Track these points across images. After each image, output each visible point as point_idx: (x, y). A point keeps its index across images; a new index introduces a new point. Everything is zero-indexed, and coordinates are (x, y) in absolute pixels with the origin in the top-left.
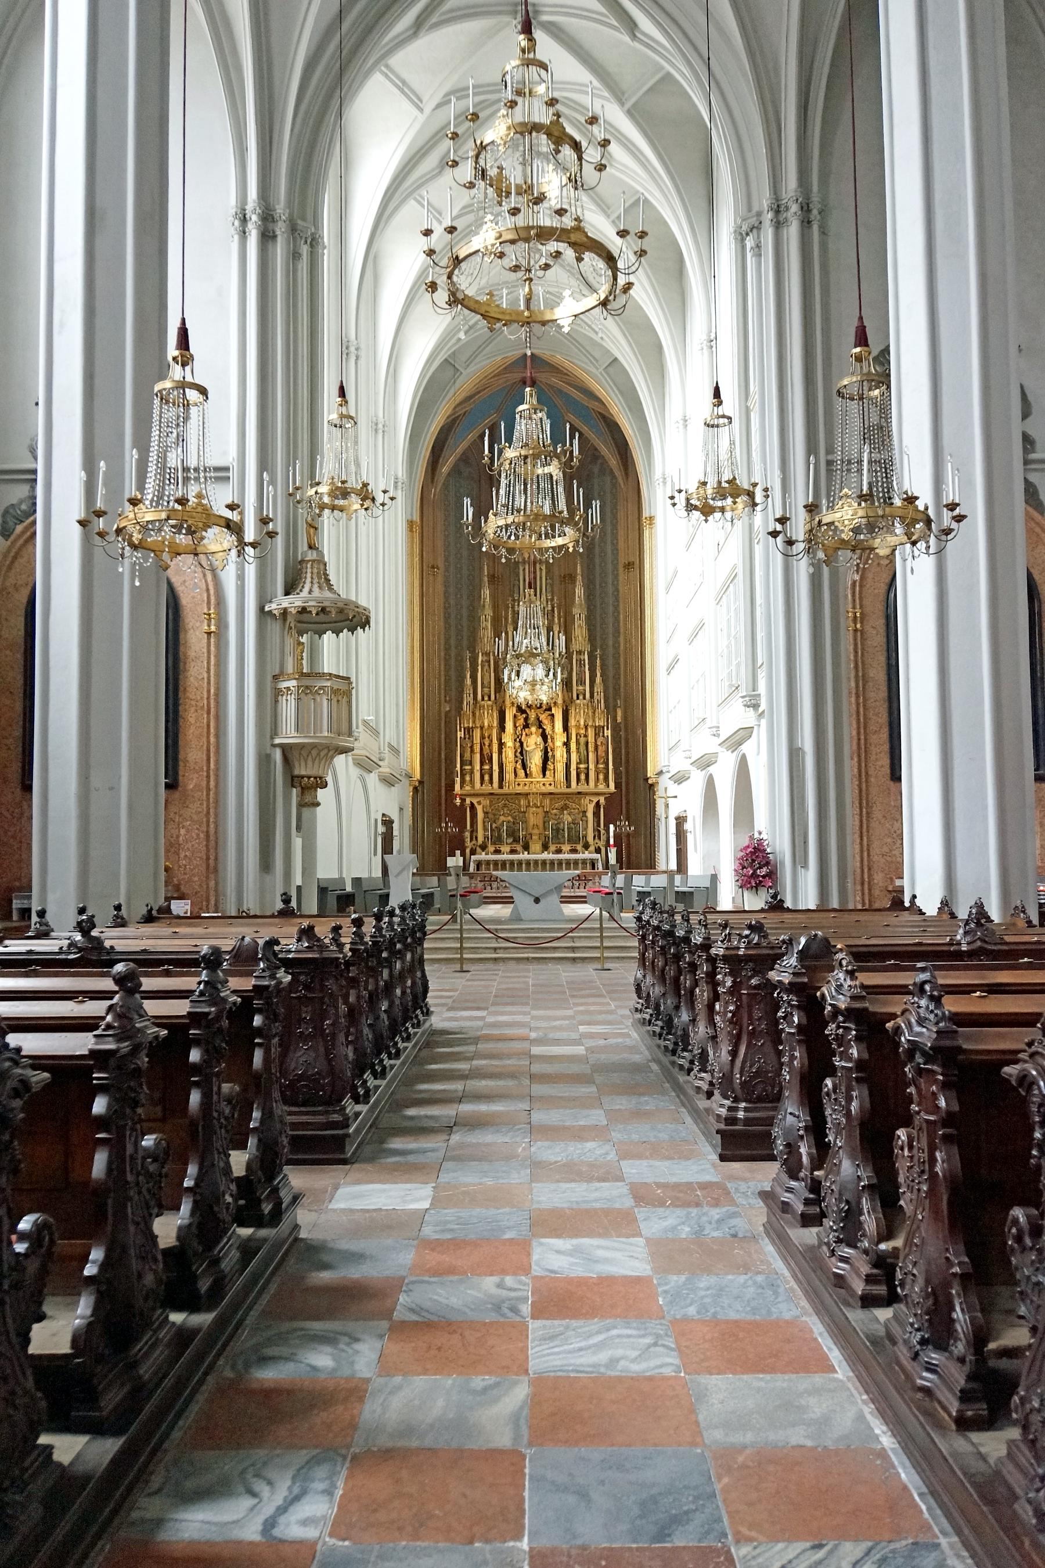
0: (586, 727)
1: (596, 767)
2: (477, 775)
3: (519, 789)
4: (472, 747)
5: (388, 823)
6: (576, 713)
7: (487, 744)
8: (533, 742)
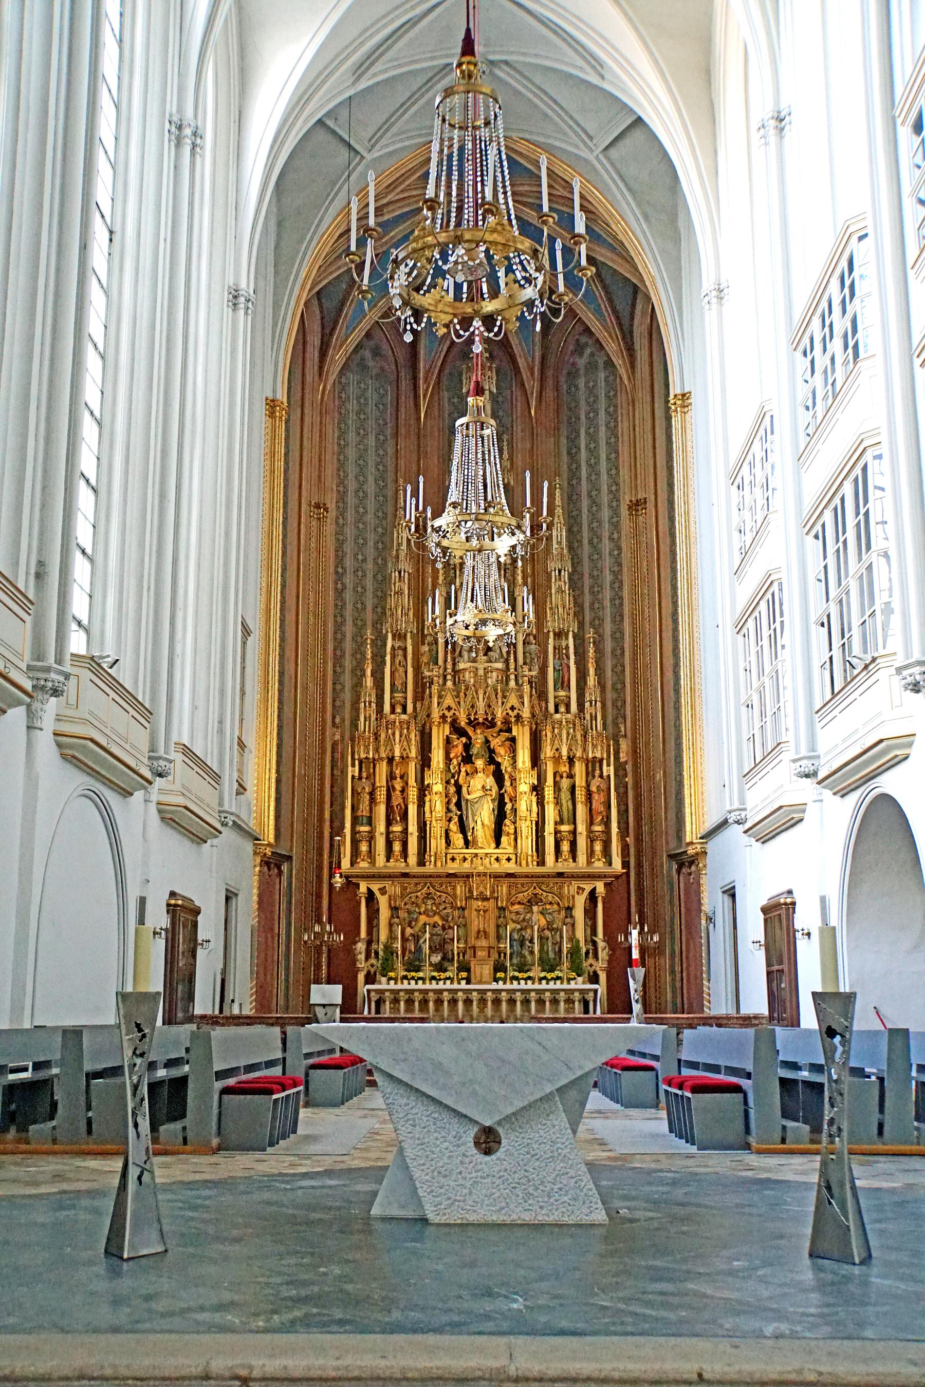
0: (571, 761)
1: (590, 831)
2: (380, 842)
3: (453, 868)
4: (372, 794)
5: (183, 914)
7: (398, 787)
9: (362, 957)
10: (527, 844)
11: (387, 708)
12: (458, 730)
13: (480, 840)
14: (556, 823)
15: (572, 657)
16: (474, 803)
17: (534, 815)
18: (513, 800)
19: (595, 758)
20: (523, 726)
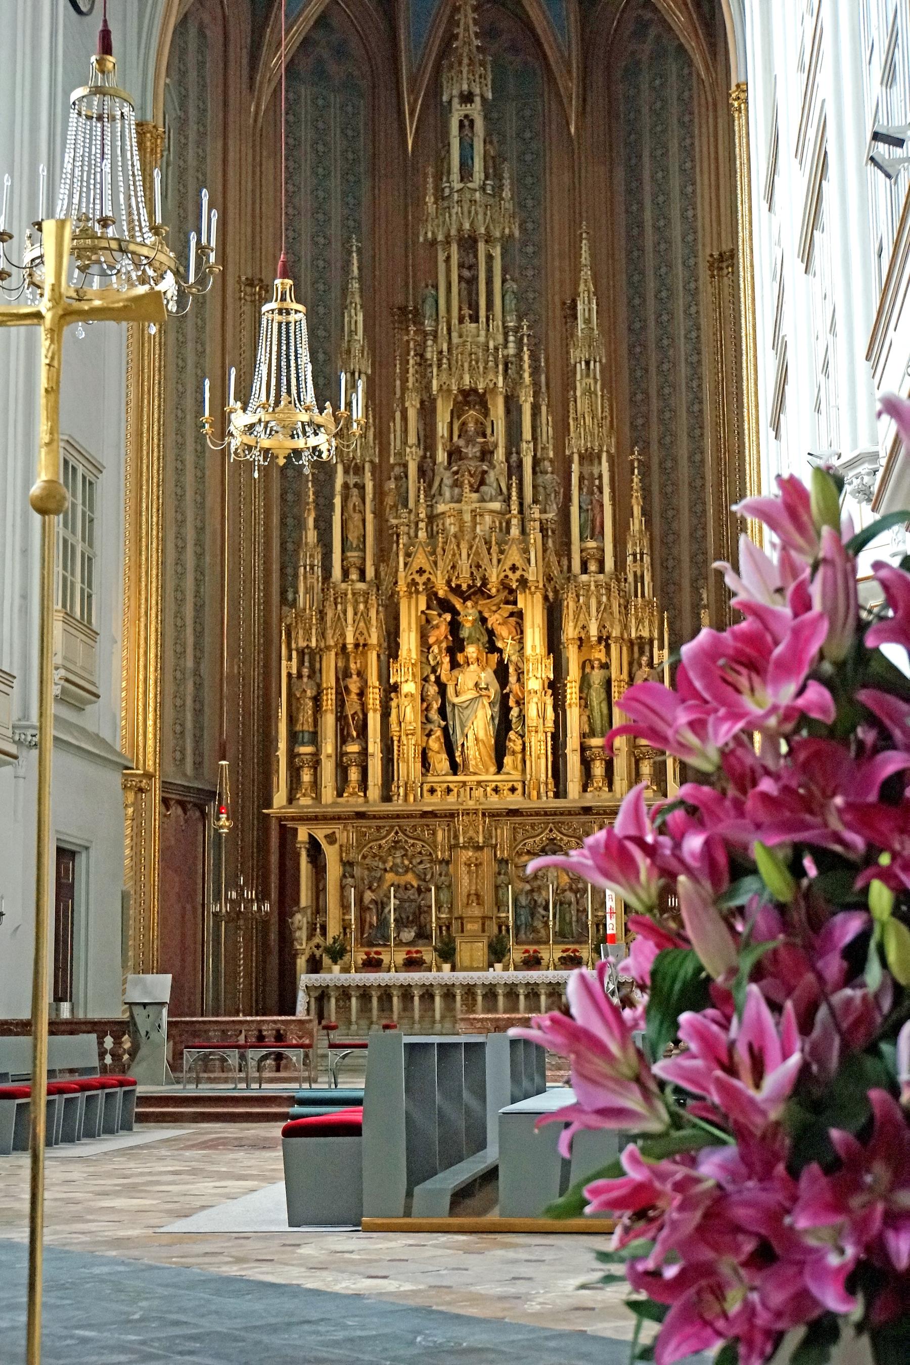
2: (328, 769)
3: (432, 803)
4: (317, 700)
6: (579, 608)
7: (354, 687)
9: (302, 934)
10: (540, 766)
13: (472, 763)
14: (583, 736)
15: (607, 490)
17: (550, 724)
18: (520, 703)
19: (641, 638)
20: (532, 594)
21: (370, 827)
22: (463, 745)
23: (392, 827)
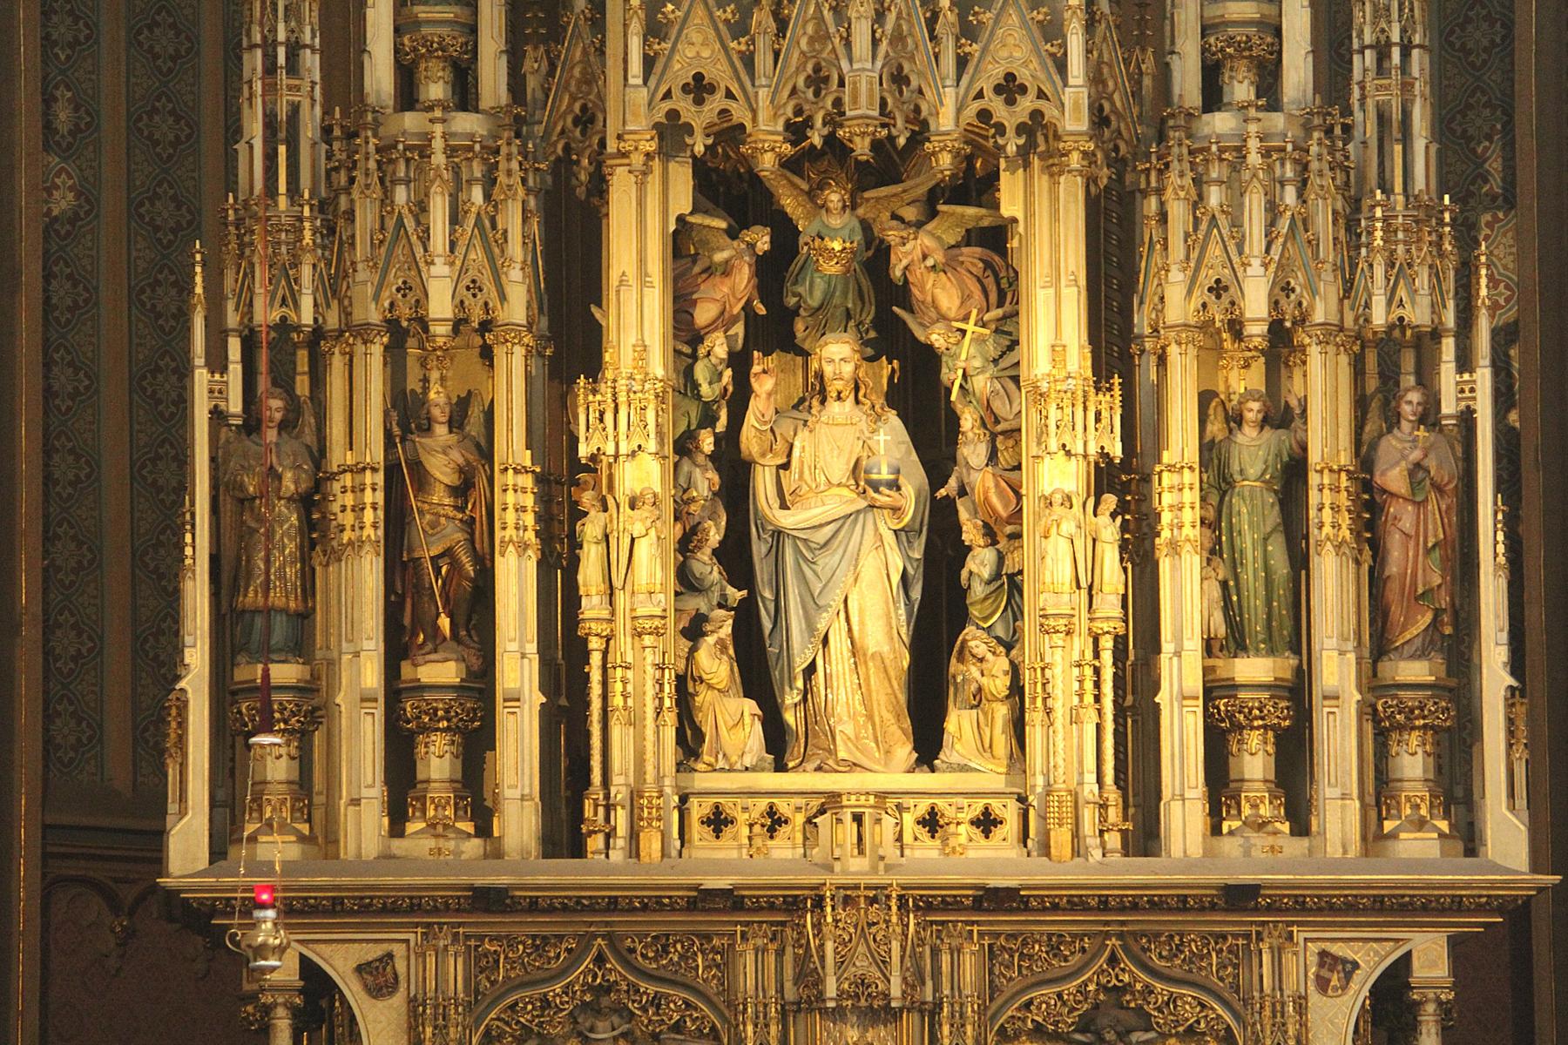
1: (1373, 684)
3: (721, 861)
4: (312, 502)
7: (442, 465)
8: (834, 457)
10: (1073, 746)
11: (380, 76)
12: (728, 187)
13: (845, 728)
14: (1209, 647)
16: (810, 550)
17: (1109, 606)
18: (1005, 530)
20: (1054, 171)
21: (512, 942)
22: (811, 670)
23: (586, 940)
